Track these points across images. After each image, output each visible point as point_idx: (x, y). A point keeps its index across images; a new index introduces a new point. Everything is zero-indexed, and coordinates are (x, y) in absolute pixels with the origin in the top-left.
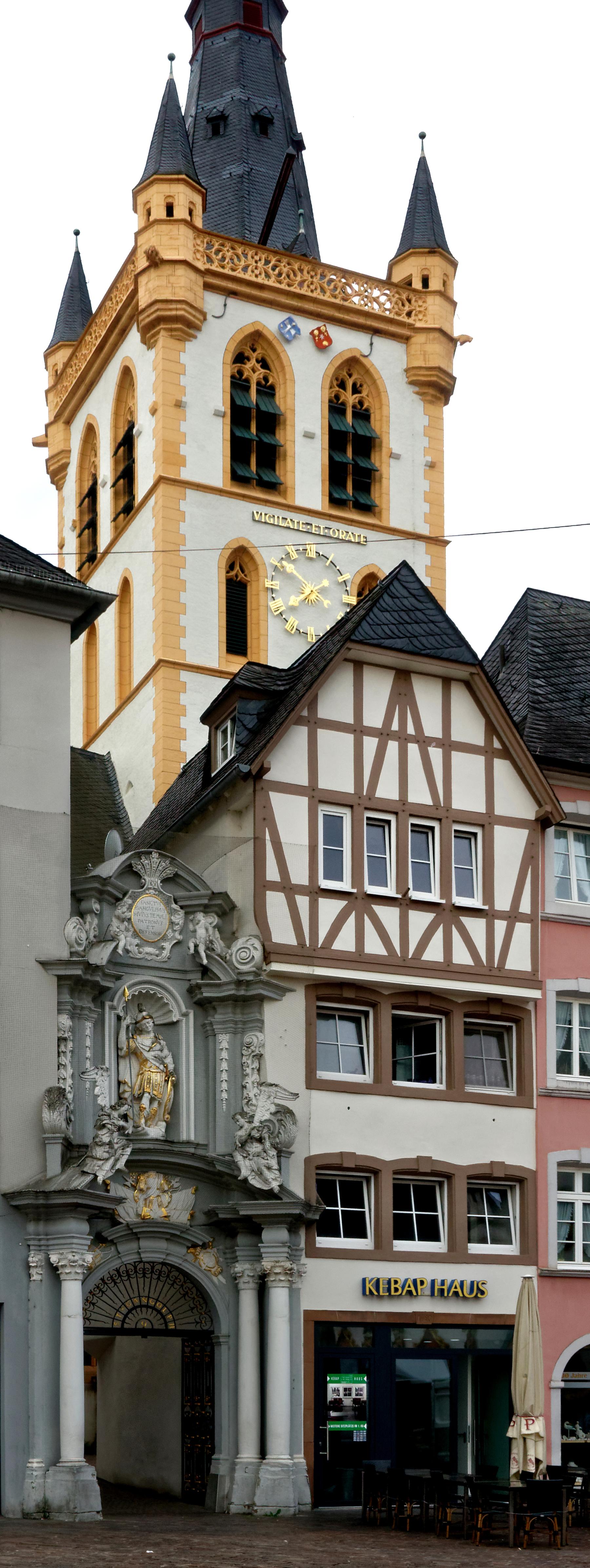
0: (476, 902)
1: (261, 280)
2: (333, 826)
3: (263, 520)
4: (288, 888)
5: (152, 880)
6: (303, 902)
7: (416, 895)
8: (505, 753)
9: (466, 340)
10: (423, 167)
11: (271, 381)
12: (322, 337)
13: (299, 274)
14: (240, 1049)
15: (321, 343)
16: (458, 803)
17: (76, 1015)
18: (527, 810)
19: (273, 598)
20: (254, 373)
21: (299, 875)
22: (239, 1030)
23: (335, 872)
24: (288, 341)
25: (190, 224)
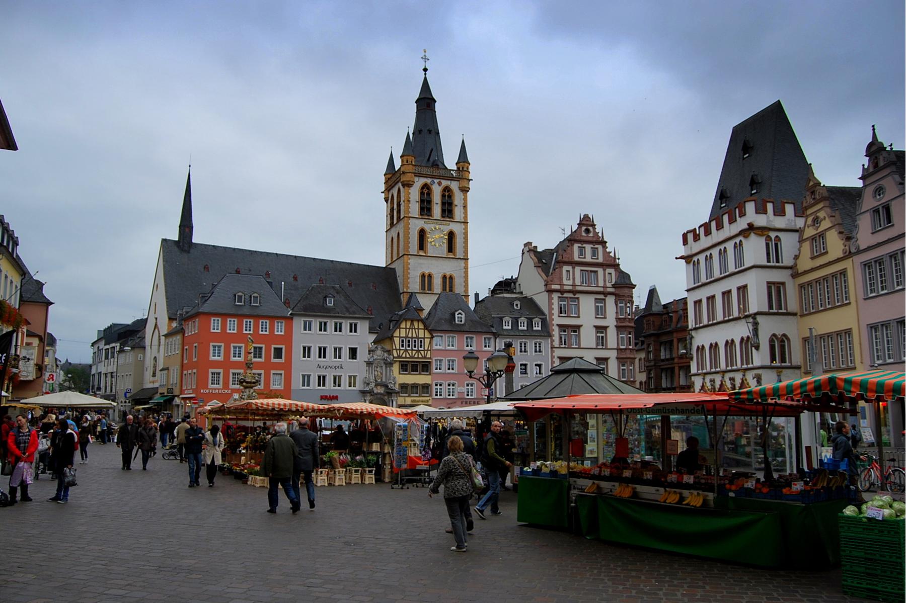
0: (422, 349)
1: (427, 173)
2: (403, 341)
4: (396, 349)
5: (379, 349)
6: (398, 351)
7: (414, 349)
8: (427, 329)
9: (471, 180)
10: (463, 141)
14: (390, 370)
15: (440, 184)
16: (420, 336)
17: (369, 367)
18: (430, 336)
20: (426, 191)
21: (398, 348)
22: (390, 367)
23: (403, 346)
24: (432, 185)
25: (412, 164)
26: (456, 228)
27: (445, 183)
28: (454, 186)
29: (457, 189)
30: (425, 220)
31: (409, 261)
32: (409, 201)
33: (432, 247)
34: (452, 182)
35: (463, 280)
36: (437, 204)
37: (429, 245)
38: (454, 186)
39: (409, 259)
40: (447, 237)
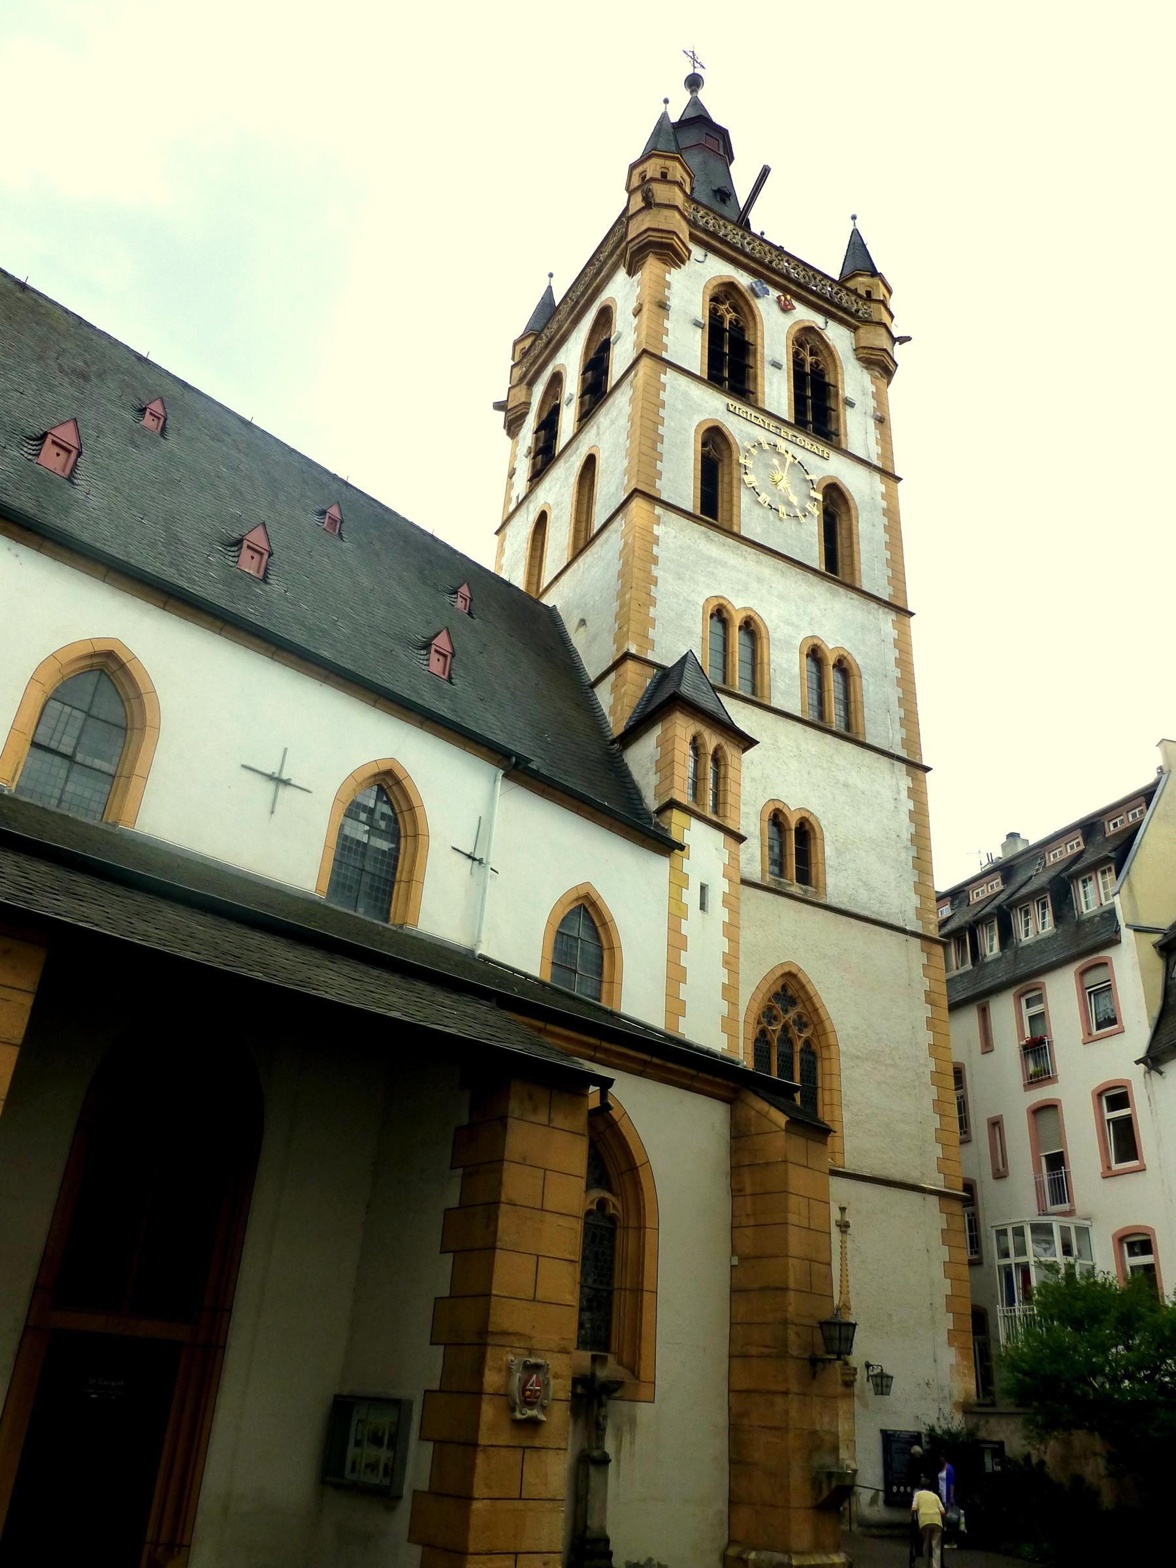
3: (737, 413)
11: (742, 324)
12: (787, 303)
13: (769, 255)
15: (786, 309)
19: (746, 473)
24: (757, 296)
26: (856, 483)
27: (803, 314)
28: (838, 337)
29: (851, 356)
30: (730, 402)
31: (658, 530)
32: (663, 306)
33: (758, 511)
34: (830, 322)
35: (894, 694)
36: (777, 365)
37: (745, 499)
38: (838, 337)
39: (658, 520)
40: (820, 497)
